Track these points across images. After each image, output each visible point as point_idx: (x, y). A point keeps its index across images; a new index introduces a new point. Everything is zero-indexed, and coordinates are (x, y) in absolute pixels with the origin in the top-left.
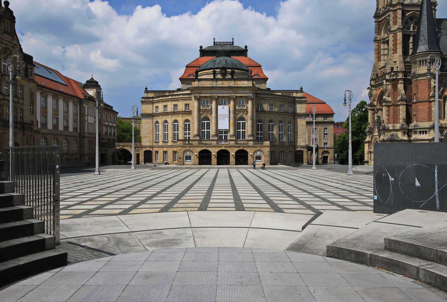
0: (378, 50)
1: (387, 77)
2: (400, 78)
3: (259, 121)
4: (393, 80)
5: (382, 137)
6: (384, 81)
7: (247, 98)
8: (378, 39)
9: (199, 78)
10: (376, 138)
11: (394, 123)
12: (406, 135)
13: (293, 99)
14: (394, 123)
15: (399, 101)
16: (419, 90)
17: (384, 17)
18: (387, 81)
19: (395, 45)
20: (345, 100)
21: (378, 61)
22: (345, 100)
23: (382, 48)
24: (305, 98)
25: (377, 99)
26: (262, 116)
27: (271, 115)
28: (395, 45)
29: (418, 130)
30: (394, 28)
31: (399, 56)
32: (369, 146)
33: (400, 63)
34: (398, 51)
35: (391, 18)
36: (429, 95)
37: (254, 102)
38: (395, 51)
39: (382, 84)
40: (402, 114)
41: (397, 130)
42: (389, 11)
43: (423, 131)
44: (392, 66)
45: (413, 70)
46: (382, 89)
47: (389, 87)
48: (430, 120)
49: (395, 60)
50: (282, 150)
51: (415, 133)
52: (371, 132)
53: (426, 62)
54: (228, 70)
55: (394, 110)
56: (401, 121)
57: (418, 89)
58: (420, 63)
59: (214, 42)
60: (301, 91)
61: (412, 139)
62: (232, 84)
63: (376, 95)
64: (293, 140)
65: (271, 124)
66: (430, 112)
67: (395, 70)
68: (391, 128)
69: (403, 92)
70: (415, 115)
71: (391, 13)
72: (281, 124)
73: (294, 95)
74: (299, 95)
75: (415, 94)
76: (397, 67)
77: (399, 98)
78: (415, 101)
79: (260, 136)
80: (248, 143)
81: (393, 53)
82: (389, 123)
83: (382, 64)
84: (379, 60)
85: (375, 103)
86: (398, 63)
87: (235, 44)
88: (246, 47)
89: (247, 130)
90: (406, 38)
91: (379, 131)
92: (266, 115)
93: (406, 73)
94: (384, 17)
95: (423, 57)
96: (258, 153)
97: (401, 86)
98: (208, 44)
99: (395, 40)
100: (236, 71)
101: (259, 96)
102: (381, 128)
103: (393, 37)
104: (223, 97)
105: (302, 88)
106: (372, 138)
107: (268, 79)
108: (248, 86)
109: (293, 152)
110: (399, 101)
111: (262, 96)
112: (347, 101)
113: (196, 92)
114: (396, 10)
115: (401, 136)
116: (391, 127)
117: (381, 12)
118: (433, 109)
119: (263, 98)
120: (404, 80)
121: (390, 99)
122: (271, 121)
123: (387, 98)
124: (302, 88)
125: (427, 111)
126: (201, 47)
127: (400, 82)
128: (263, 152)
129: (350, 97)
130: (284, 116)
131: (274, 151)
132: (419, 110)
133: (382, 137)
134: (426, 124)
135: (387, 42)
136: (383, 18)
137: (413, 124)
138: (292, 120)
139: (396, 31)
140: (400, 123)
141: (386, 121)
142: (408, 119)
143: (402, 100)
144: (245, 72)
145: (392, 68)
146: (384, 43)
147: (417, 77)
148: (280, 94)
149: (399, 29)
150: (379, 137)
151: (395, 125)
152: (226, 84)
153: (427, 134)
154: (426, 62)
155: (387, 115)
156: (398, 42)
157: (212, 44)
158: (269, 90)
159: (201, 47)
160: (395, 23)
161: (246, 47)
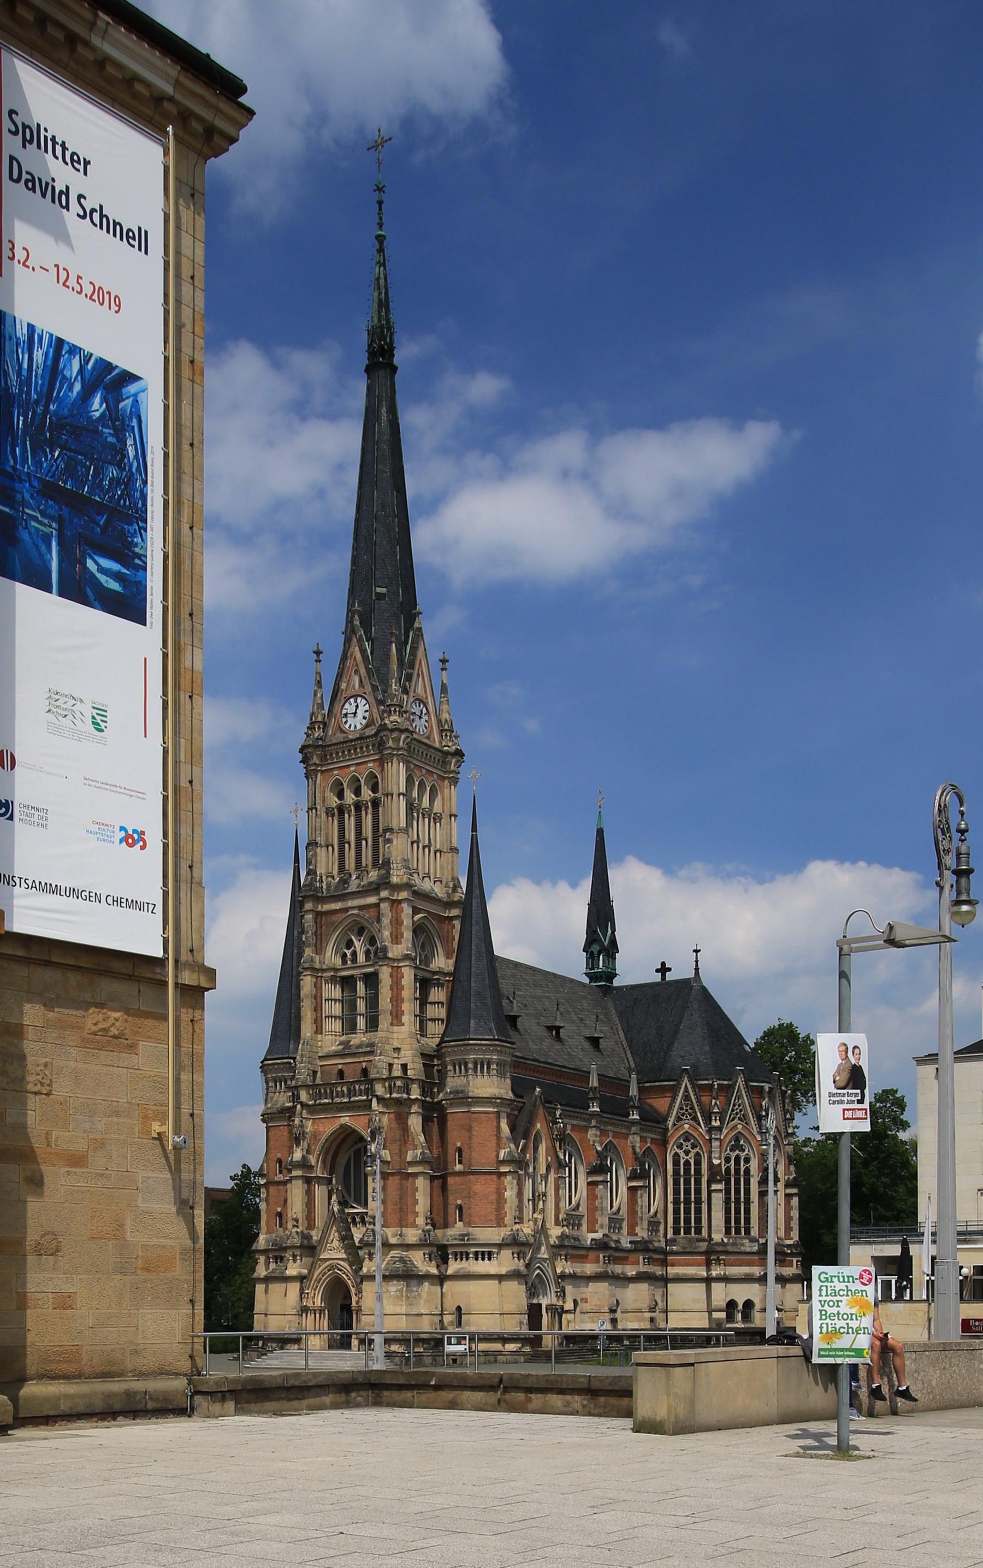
2: (417, 1099)
4: (398, 1102)
6: (374, 1100)
11: (401, 1227)
15: (411, 1164)
16: (475, 1140)
18: (380, 1100)
19: (397, 1000)
21: (316, 1032)
25: (318, 1147)
28: (397, 1000)
30: (395, 951)
34: (405, 1019)
35: (386, 921)
36: (498, 1156)
38: (397, 1017)
41: (408, 1247)
43: (483, 1253)
45: (453, 1082)
47: (385, 1119)
49: (396, 1045)
51: (464, 1256)
53: (489, 1067)
55: (401, 1188)
56: (420, 1221)
57: (470, 1138)
58: (476, 1067)
61: (449, 1272)
63: (315, 1135)
66: (500, 1201)
68: (393, 1241)
69: (422, 1138)
70: (460, 1208)
75: (460, 1151)
76: (404, 1067)
78: (458, 1167)
81: (392, 1024)
83: (330, 1042)
84: (319, 1030)
85: (312, 1160)
93: (426, 1088)
95: (484, 1052)
97: (415, 1122)
103: (391, 976)
106: (311, 1269)
110: (411, 1164)
115: (421, 1262)
116: (392, 1236)
117: (324, 885)
120: (424, 1104)
121: (386, 1155)
125: (493, 1197)
127: (415, 1108)
132: (475, 1194)
134: (492, 1235)
137: (451, 1232)
139: (399, 960)
140: (414, 1225)
142: (439, 1219)
145: (391, 1065)
146: (333, 980)
147: (469, 1105)
149: (406, 957)
153: (494, 1262)
154: (489, 1067)
160: (396, 938)
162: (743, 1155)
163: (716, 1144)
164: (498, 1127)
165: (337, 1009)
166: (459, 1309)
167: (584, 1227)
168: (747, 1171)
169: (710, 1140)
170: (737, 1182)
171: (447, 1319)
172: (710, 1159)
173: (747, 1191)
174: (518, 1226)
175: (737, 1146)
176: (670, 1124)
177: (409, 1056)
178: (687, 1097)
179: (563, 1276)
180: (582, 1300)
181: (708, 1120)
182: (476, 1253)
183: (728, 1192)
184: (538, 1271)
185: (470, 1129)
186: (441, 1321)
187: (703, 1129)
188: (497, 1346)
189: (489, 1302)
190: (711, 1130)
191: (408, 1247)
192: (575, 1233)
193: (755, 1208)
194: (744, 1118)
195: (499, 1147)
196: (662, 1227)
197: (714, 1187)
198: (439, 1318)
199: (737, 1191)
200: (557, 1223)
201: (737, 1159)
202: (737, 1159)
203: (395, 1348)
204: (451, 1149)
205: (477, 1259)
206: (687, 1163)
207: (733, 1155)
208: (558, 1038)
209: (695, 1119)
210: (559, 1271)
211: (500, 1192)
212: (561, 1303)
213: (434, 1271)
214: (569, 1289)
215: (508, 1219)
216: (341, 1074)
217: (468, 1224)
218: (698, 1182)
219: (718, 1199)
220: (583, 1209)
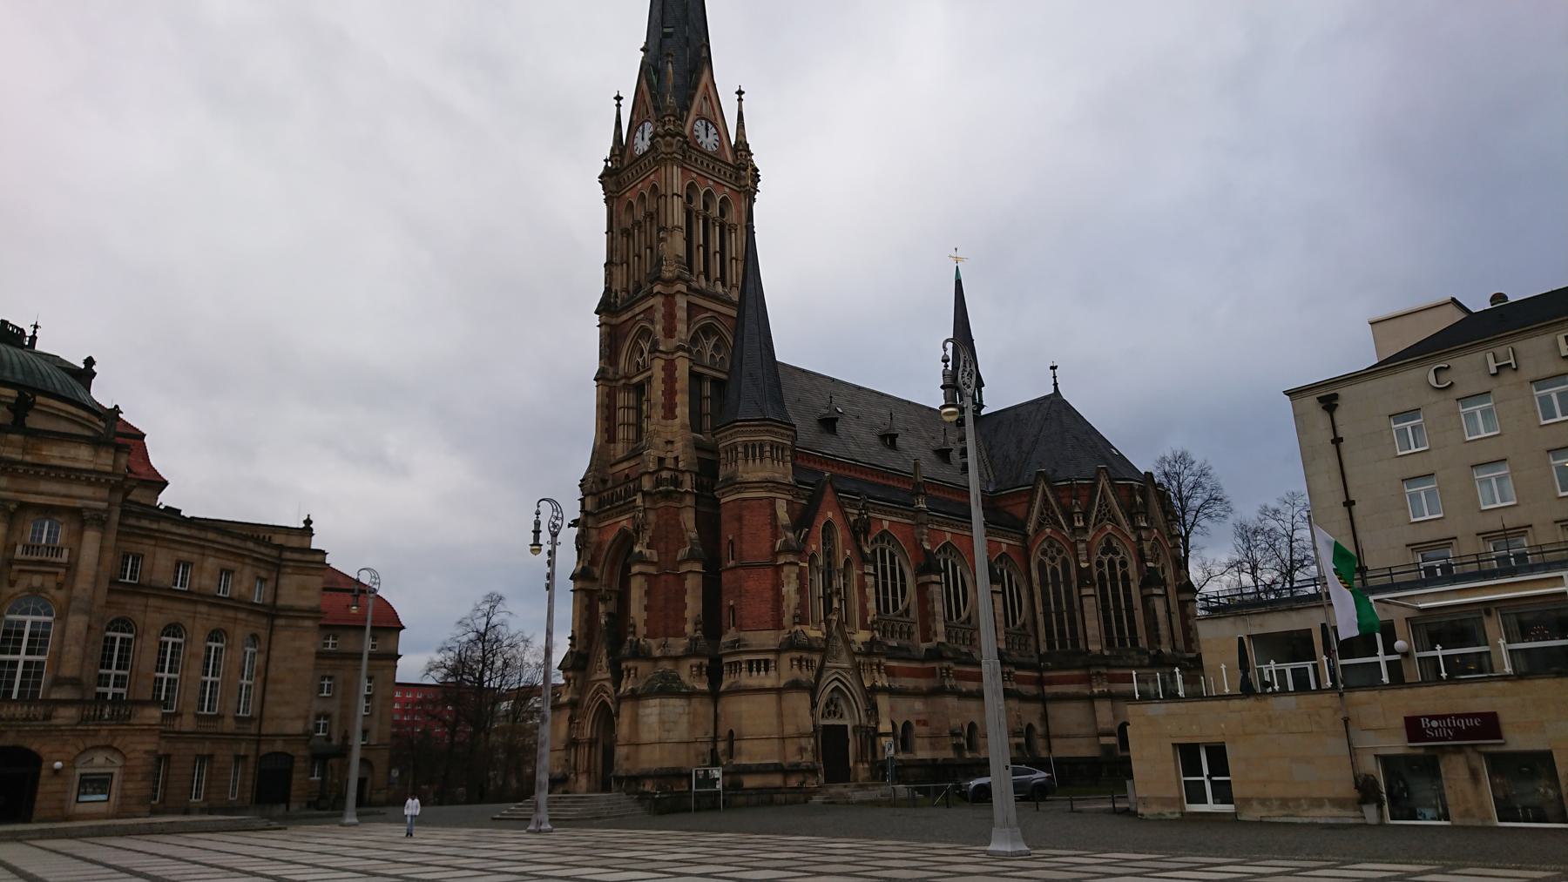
0: (608, 407)
1: (647, 483)
3: (124, 624)
5: (626, 686)
6: (639, 500)
7: (80, 518)
8: (610, 375)
10: (602, 688)
12: (705, 677)
13: (275, 553)
14: (667, 636)
17: (630, 314)
19: (670, 393)
20: (537, 532)
22: (537, 532)
23: (620, 403)
24: (323, 553)
26: (134, 607)
27: (183, 606)
28: (670, 393)
29: (746, 657)
31: (683, 426)
32: (571, 720)
33: (685, 446)
34: (678, 411)
37: (112, 537)
39: (630, 507)
40: (693, 605)
42: (651, 294)
43: (758, 662)
44: (662, 455)
45: (723, 472)
46: (624, 521)
48: (778, 626)
49: (670, 438)
50: (206, 748)
56: (689, 628)
63: (599, 545)
64: (257, 710)
65: (171, 640)
66: (778, 598)
67: (669, 463)
68: (657, 653)
69: (694, 535)
71: (657, 302)
72: (213, 645)
73: (278, 539)
74: (295, 542)
75: (732, 542)
76: (676, 459)
77: (683, 552)
79: (110, 691)
80: (48, 717)
86: (679, 445)
88: (90, 362)
89: (57, 659)
90: (695, 377)
92: (152, 602)
94: (630, 314)
96: (100, 759)
99: (670, 378)
100: (39, 399)
101: (132, 521)
102: (626, 650)
105: (308, 522)
107: (166, 483)
108: (91, 466)
109: (251, 759)
111: (145, 523)
112: (545, 537)
114: (673, 296)
118: (784, 590)
119: (148, 534)
122: (173, 629)
123: (647, 552)
124: (308, 522)
125: (769, 595)
128: (124, 757)
129: (555, 526)
130: (230, 614)
131: (167, 757)
133: (626, 686)
135: (640, 389)
136: (625, 317)
138: (263, 633)
141: (642, 629)
142: (712, 622)
143: (691, 557)
144: (83, 414)
146: (626, 387)
150: (617, 685)
151: (671, 640)
153: (772, 673)
155: (646, 608)
156: (678, 386)
158: (173, 513)
161: (90, 362)
162: (1117, 559)
163: (1081, 546)
164: (774, 515)
165: (632, 416)
166: (731, 732)
167: (917, 635)
168: (1125, 576)
169: (1074, 546)
170: (1115, 588)
171: (721, 746)
172: (1077, 562)
173: (1128, 597)
174: (798, 627)
175: (1109, 548)
176: (1031, 528)
177: (679, 445)
178: (1045, 499)
180: (918, 722)
181: (1071, 522)
182: (750, 662)
183: (1104, 598)
184: (837, 683)
185: (740, 519)
186: (714, 751)
187: (1066, 532)
188: (777, 780)
189: (767, 723)
190: (1074, 530)
191: (677, 659)
192: (905, 642)
193: (1139, 615)
194: (1114, 519)
195: (775, 536)
196: (1032, 641)
197: (1085, 591)
198: (710, 746)
199: (1116, 598)
200: (864, 626)
201: (1112, 563)
202: (1112, 563)
203: (648, 787)
204: (724, 543)
205: (751, 670)
206: (1054, 570)
207: (1106, 560)
208: (893, 446)
209: (1057, 522)
210: (867, 684)
212: (873, 724)
213: (705, 687)
215: (787, 620)
216: (627, 476)
217: (740, 628)
218: (1069, 592)
219: (1089, 604)
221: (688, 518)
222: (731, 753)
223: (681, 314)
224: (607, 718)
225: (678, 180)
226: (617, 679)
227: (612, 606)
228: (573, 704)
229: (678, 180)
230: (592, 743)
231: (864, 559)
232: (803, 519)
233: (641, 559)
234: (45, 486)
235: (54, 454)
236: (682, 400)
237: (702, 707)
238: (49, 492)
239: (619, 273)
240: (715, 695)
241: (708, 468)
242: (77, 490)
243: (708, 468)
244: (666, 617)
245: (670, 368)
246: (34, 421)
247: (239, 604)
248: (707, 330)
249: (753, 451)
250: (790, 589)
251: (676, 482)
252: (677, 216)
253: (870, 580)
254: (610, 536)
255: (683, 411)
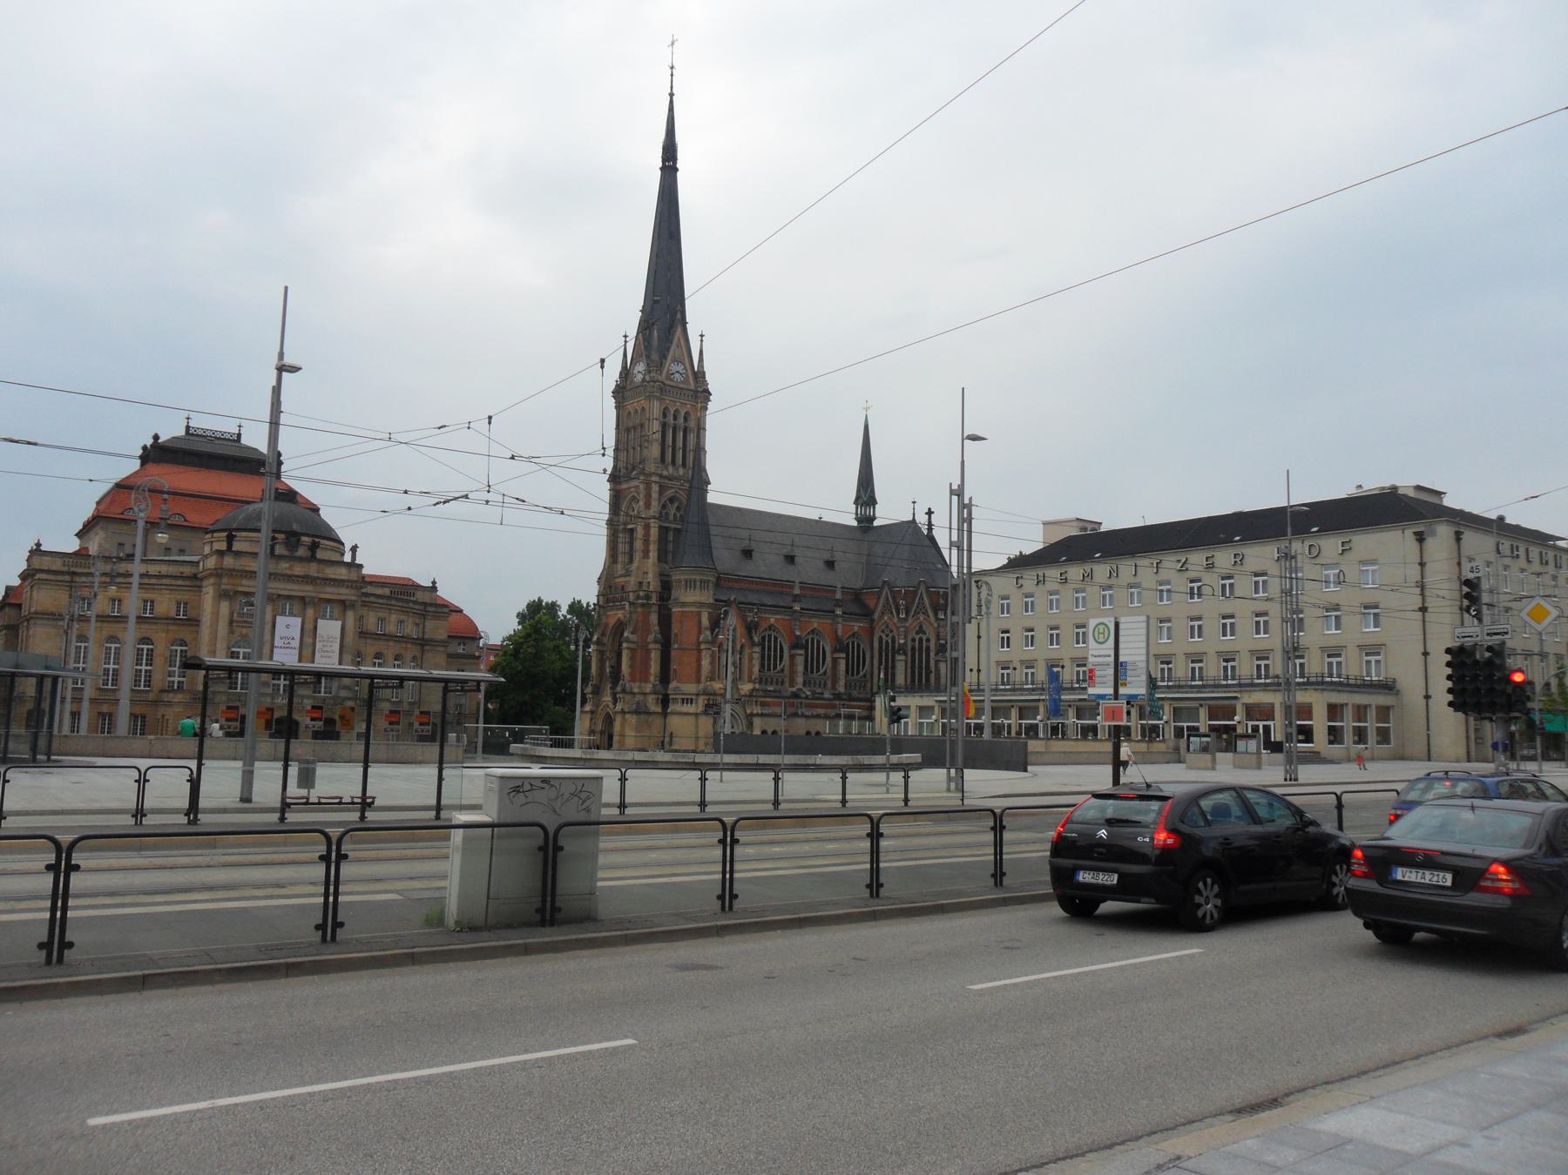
5: (619, 707)
9: (237, 546)
19: (646, 541)
28: (646, 541)
38: (646, 553)
40: (655, 668)
45: (674, 594)
46: (620, 614)
48: (698, 681)
52: (597, 691)
54: (304, 539)
59: (188, 427)
60: (434, 588)
62: (313, 570)
82: (633, 680)
87: (244, 441)
90: (663, 530)
91: (614, 696)
98: (171, 430)
102: (619, 689)
104: (289, 597)
113: (225, 580)
121: (632, 637)
126: (156, 437)
134: (691, 688)
141: (627, 677)
142: (665, 677)
148: (387, 591)
152: (299, 570)
157: (182, 432)
159: (156, 437)
160: (648, 506)
179: (752, 715)
195: (700, 633)
200: (750, 681)
211: (699, 661)
214: (757, 721)
220: (786, 672)
221: (654, 618)
222: (671, 743)
223: (655, 495)
224: (609, 720)
225: (661, 391)
226: (615, 701)
227: (613, 662)
228: (592, 712)
229: (661, 391)
230: (602, 732)
231: (753, 644)
232: (715, 624)
233: (628, 641)
234: (329, 589)
235: (331, 572)
236: (653, 548)
237: (659, 721)
238: (330, 592)
239: (623, 456)
240: (665, 714)
241: (666, 586)
242: (344, 591)
243: (666, 586)
244: (641, 673)
245: (647, 527)
246: (320, 554)
247: (404, 639)
248: (672, 500)
249: (690, 584)
250: (705, 663)
251: (648, 597)
252: (656, 426)
253: (756, 656)
254: (612, 622)
255: (653, 555)
